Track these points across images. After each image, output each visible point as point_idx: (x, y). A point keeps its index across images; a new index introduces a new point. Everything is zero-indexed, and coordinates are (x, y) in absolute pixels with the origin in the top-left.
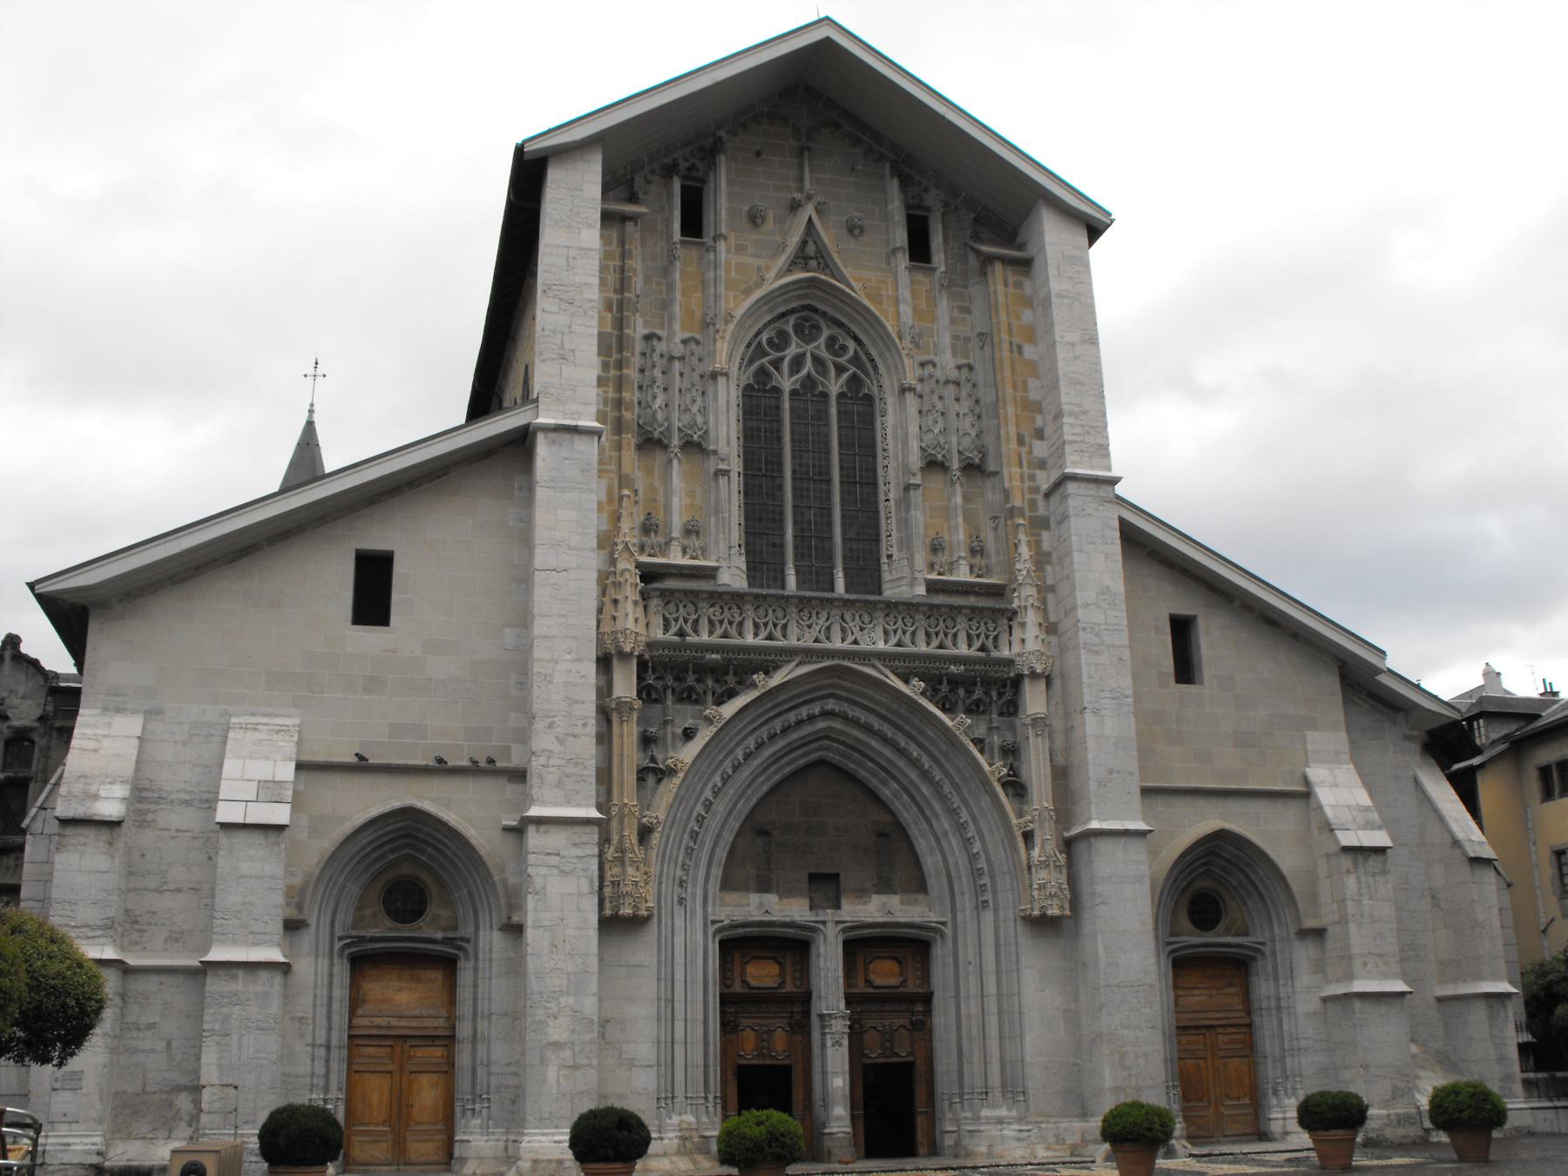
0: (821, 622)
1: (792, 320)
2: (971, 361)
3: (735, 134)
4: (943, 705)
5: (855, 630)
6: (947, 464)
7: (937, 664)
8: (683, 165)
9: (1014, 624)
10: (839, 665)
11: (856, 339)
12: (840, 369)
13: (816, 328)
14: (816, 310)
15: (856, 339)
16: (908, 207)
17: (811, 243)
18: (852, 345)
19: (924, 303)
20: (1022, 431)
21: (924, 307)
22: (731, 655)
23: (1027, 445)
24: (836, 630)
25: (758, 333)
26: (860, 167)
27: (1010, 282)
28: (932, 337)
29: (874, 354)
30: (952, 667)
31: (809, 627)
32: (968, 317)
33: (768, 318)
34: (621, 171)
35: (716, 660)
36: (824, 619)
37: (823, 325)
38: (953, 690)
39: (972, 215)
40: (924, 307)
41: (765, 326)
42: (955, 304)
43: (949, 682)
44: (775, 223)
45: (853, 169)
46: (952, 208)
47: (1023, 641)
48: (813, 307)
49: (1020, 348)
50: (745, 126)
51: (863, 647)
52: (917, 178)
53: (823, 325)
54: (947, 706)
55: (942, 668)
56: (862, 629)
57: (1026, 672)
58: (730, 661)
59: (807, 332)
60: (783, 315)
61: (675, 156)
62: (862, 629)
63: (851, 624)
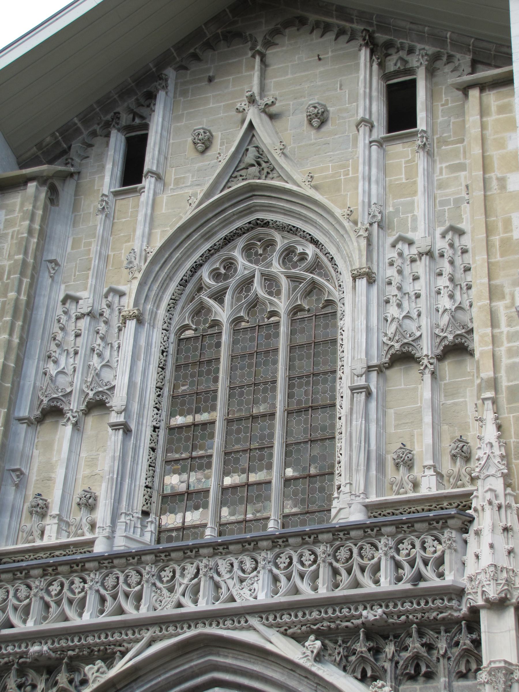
0: (186, 581)
1: (241, 242)
2: (461, 226)
3: (186, 69)
4: (364, 673)
5: (230, 583)
6: (417, 355)
7: (345, 611)
8: (125, 119)
9: (471, 537)
10: (200, 635)
11: (315, 242)
12: (294, 279)
13: (270, 244)
14: (266, 224)
15: (315, 242)
16: (386, 76)
17: (252, 149)
18: (310, 250)
19: (403, 176)
20: (496, 282)
21: (404, 181)
22: (63, 643)
23: (508, 297)
24: (205, 586)
25: (196, 268)
26: (330, 54)
27: (493, 108)
28: (412, 211)
29: (332, 250)
30: (365, 613)
31: (171, 590)
32: (463, 174)
33: (207, 246)
34: (48, 139)
35: (40, 654)
36: (189, 576)
37: (277, 237)
38: (376, 651)
39: (468, 58)
40: (404, 181)
41: (206, 258)
42: (444, 165)
43: (368, 637)
44: (222, 144)
45: (320, 59)
46: (445, 59)
47: (477, 557)
48: (263, 220)
49: (502, 182)
50: (195, 57)
51: (239, 603)
52: (398, 41)
53: (277, 237)
54: (369, 674)
55: (353, 617)
56: (242, 581)
57: (480, 602)
58: (63, 650)
59: (260, 251)
60: (228, 240)
61: (117, 110)
62: (242, 581)
63: (226, 576)
